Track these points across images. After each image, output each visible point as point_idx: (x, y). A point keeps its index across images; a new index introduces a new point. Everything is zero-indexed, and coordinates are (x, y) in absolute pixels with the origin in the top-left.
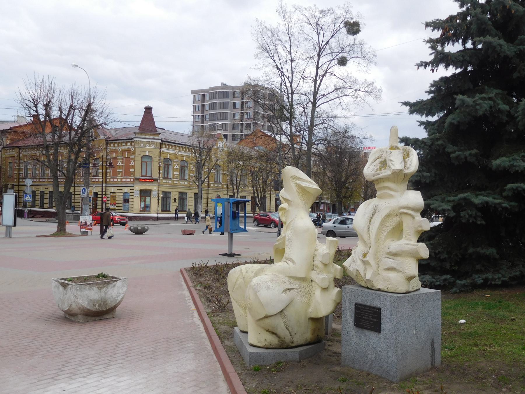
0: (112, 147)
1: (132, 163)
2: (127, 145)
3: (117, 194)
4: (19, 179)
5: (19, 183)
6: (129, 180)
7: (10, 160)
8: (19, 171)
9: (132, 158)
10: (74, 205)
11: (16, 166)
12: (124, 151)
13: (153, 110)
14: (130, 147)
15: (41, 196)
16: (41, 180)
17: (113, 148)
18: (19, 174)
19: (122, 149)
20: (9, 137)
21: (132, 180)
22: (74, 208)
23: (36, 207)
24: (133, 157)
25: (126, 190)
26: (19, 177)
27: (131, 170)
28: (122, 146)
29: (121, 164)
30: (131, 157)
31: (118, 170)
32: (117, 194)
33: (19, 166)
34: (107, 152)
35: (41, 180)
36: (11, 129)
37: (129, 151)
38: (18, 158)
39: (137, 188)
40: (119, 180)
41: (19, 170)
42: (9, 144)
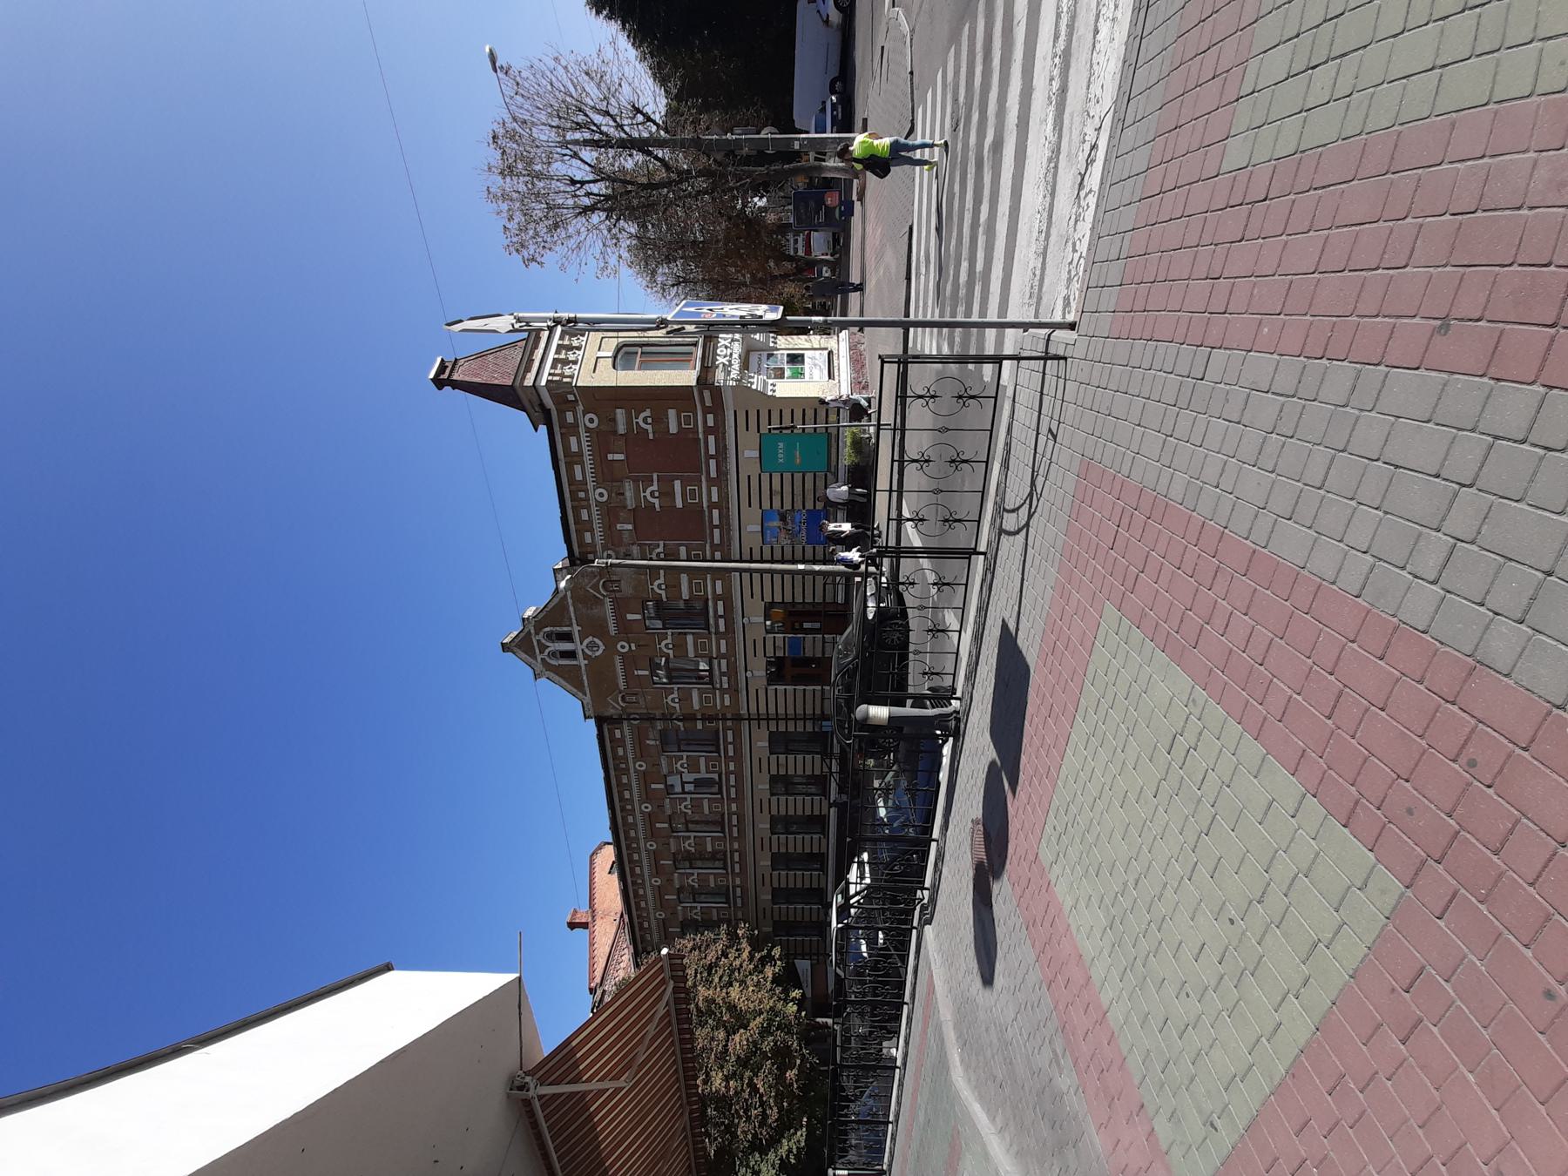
0: (595, 537)
1: (643, 420)
2: (580, 454)
3: (766, 505)
6: (711, 439)
10: (814, 718)
12: (607, 475)
14: (583, 434)
17: (599, 540)
21: (711, 423)
23: (823, 885)
24: (620, 414)
27: (673, 429)
28: (584, 482)
29: (655, 487)
30: (622, 429)
31: (679, 504)
32: (766, 505)
37: (603, 439)
40: (714, 490)
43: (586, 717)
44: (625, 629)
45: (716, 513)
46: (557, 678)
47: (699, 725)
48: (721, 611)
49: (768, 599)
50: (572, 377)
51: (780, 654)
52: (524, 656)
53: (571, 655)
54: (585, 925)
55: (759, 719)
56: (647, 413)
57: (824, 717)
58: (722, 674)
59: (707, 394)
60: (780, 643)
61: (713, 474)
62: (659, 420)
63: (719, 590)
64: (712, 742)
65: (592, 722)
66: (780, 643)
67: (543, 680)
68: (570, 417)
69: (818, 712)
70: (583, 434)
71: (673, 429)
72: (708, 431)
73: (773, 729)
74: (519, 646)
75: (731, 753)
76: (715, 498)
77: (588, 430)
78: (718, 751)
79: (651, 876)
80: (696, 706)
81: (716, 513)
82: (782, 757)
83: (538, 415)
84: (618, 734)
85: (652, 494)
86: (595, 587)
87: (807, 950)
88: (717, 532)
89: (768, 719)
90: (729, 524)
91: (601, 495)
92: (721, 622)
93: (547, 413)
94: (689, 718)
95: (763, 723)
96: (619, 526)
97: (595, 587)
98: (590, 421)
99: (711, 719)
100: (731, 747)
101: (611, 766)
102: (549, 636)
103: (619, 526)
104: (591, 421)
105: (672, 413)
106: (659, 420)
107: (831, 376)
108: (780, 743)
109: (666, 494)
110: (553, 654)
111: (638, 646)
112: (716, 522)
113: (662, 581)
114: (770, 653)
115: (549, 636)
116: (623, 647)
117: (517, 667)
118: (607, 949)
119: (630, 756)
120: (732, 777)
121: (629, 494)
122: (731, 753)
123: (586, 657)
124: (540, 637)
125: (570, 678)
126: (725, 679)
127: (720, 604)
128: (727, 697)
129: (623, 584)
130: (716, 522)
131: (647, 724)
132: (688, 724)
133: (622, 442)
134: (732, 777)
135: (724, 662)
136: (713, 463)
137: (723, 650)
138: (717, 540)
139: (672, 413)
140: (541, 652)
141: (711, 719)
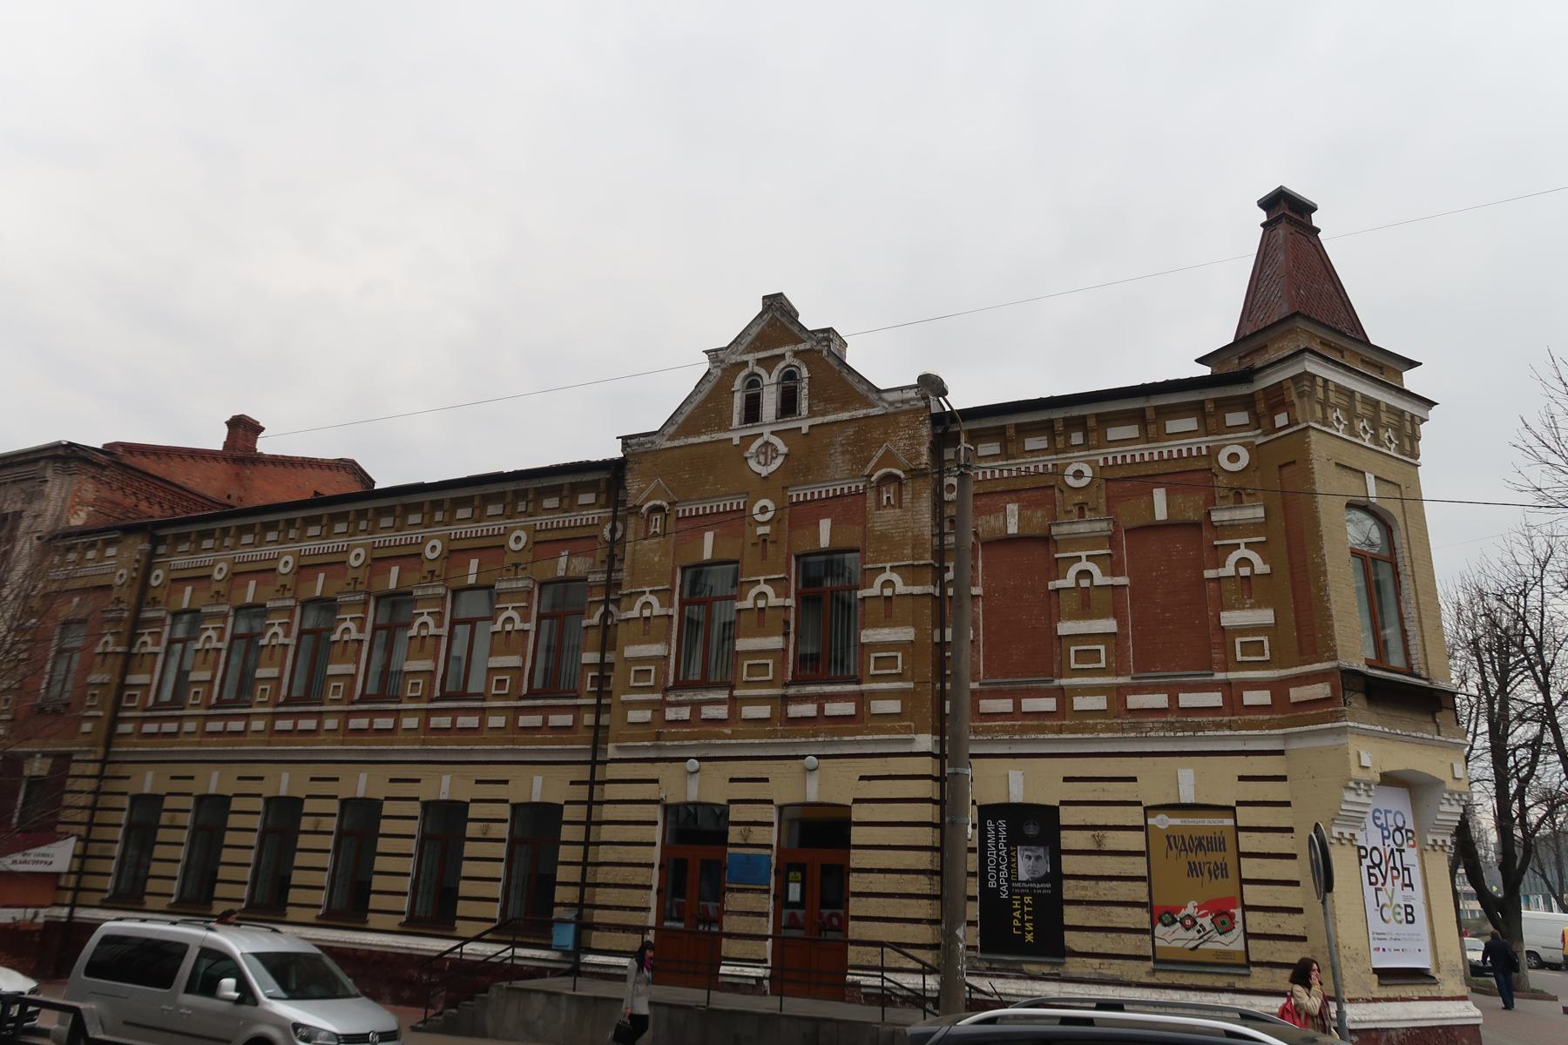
1: (1243, 559)
4: (115, 720)
5: (108, 744)
6: (1214, 699)
7: (73, 606)
8: (126, 670)
9: (1234, 528)
11: (109, 643)
12: (1125, 484)
13: (1316, 218)
14: (1202, 443)
15: (265, 833)
16: (282, 725)
18: (123, 686)
19: (1099, 471)
20: (89, 490)
21: (1251, 698)
22: (584, 927)
25: (1188, 783)
26: (117, 707)
27: (1229, 618)
29: (1099, 579)
31: (1065, 628)
33: (133, 637)
34: (939, 504)
35: (282, 725)
36: (110, 450)
37: (1193, 477)
38: (129, 597)
39: (1366, 761)
40: (1099, 703)
41: (129, 662)
42: (85, 524)
43: (626, 440)
44: (799, 515)
45: (1049, 704)
46: (707, 387)
47: (590, 657)
48: (832, 709)
49: (859, 813)
50: (1325, 421)
51: (734, 834)
52: (755, 331)
53: (752, 411)
54: (226, 444)
55: (592, 783)
56: (1261, 567)
57: (584, 927)
58: (696, 706)
59: (1321, 690)
60: (758, 835)
61: (1135, 701)
62: (1248, 589)
63: (879, 707)
64: (553, 683)
65: (616, 453)
66: (758, 835)
67: (704, 365)
68: (1236, 418)
69: (599, 916)
70: (1202, 443)
71: (1229, 618)
72: (1232, 691)
73: (569, 813)
74: (772, 323)
75: (524, 720)
76: (1081, 703)
77: (1213, 453)
78: (532, 694)
79: (299, 556)
80: (631, 651)
81: (1049, 704)
82: (503, 830)
83: (1234, 366)
84: (586, 498)
85: (1086, 574)
86: (888, 459)
87: (93, 865)
88: (1005, 705)
89: (590, 803)
90: (1024, 730)
91: (1079, 474)
92: (809, 710)
93: (1247, 376)
94: (607, 638)
95: (582, 793)
96: (1012, 508)
97: (888, 459)
98: (1233, 455)
99: (602, 680)
100: (536, 720)
101: (523, 485)
102: (790, 375)
103: (1012, 508)
104: (1234, 457)
105: (1266, 616)
106: (1248, 589)
107: (1387, 976)
108: (536, 825)
109: (1087, 603)
110: (753, 382)
111: (764, 539)
112: (1029, 704)
113: (901, 588)
114: (736, 813)
115: (790, 375)
116: (763, 509)
117: (732, 318)
118: (179, 479)
119: (540, 521)
120: (473, 721)
121: (1083, 528)
122: (524, 720)
123: (747, 441)
124: (789, 360)
125: (703, 409)
126: (685, 713)
127: (848, 708)
128: (646, 715)
129: (889, 514)
130: (1029, 704)
131: (601, 554)
132: (594, 636)
133: (1191, 515)
134: (473, 721)
135: (721, 712)
136: (1160, 700)
137: (749, 712)
138: (988, 705)
139: (1266, 616)
140: (759, 362)
141: (602, 680)
